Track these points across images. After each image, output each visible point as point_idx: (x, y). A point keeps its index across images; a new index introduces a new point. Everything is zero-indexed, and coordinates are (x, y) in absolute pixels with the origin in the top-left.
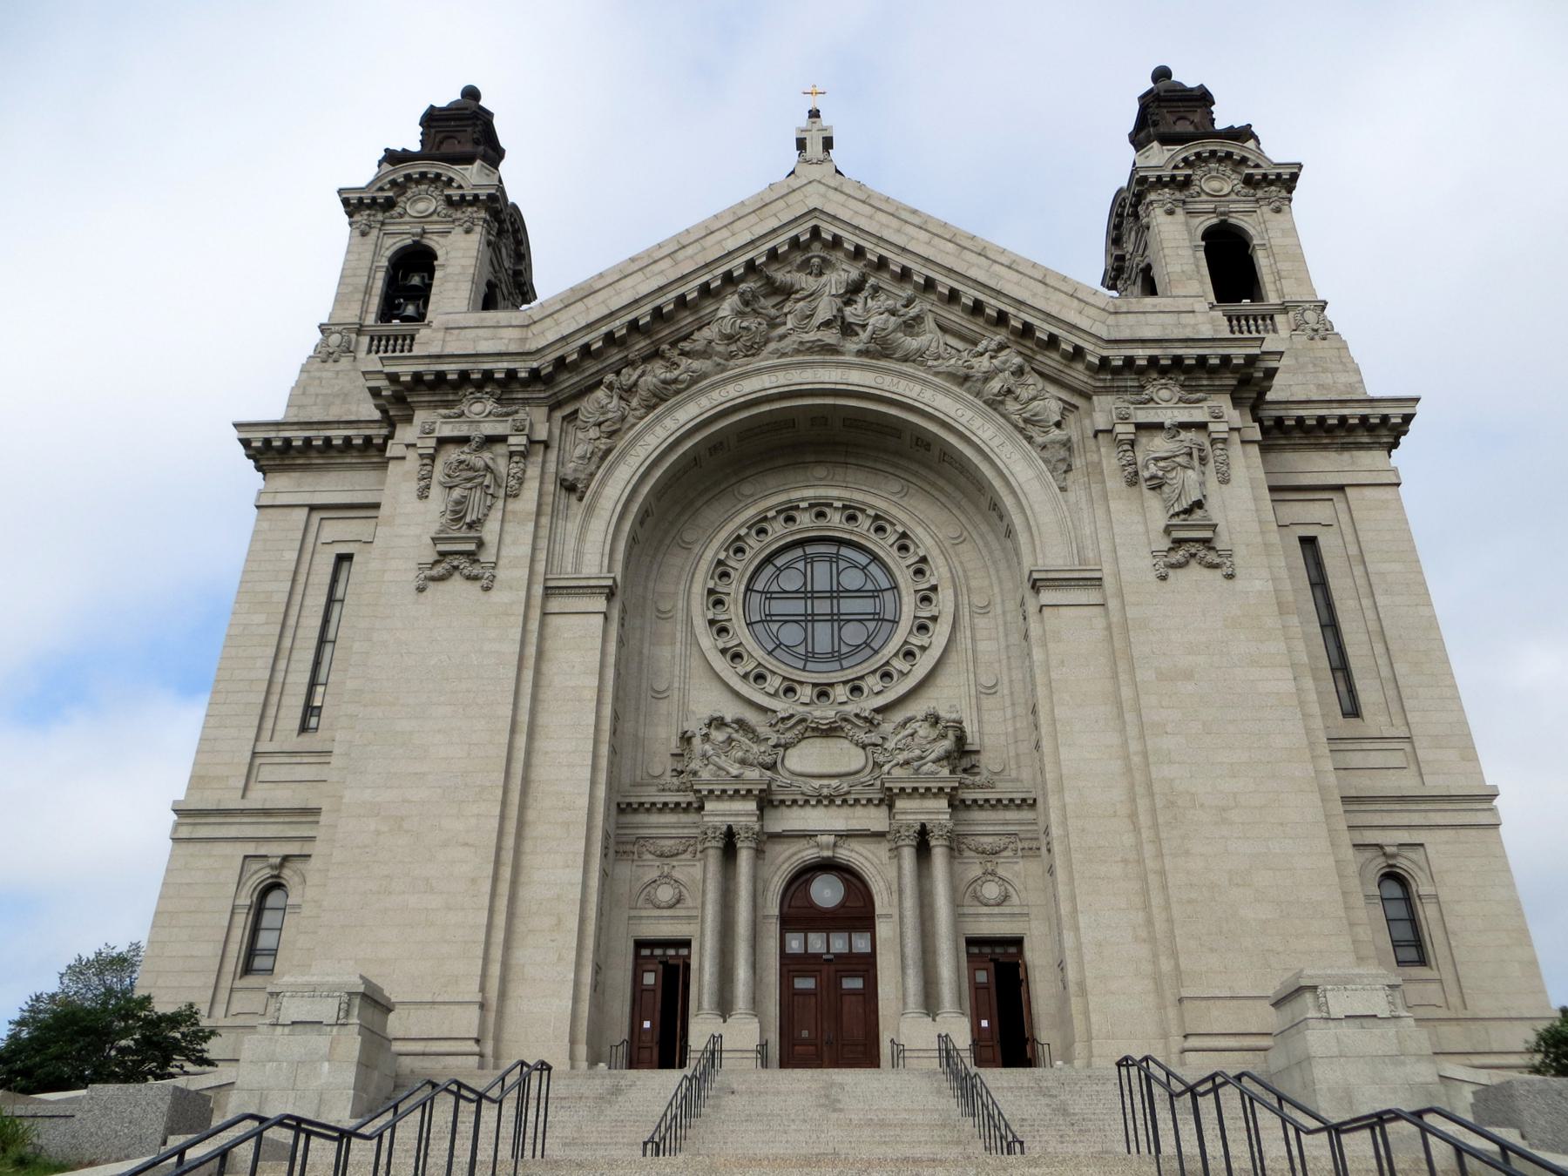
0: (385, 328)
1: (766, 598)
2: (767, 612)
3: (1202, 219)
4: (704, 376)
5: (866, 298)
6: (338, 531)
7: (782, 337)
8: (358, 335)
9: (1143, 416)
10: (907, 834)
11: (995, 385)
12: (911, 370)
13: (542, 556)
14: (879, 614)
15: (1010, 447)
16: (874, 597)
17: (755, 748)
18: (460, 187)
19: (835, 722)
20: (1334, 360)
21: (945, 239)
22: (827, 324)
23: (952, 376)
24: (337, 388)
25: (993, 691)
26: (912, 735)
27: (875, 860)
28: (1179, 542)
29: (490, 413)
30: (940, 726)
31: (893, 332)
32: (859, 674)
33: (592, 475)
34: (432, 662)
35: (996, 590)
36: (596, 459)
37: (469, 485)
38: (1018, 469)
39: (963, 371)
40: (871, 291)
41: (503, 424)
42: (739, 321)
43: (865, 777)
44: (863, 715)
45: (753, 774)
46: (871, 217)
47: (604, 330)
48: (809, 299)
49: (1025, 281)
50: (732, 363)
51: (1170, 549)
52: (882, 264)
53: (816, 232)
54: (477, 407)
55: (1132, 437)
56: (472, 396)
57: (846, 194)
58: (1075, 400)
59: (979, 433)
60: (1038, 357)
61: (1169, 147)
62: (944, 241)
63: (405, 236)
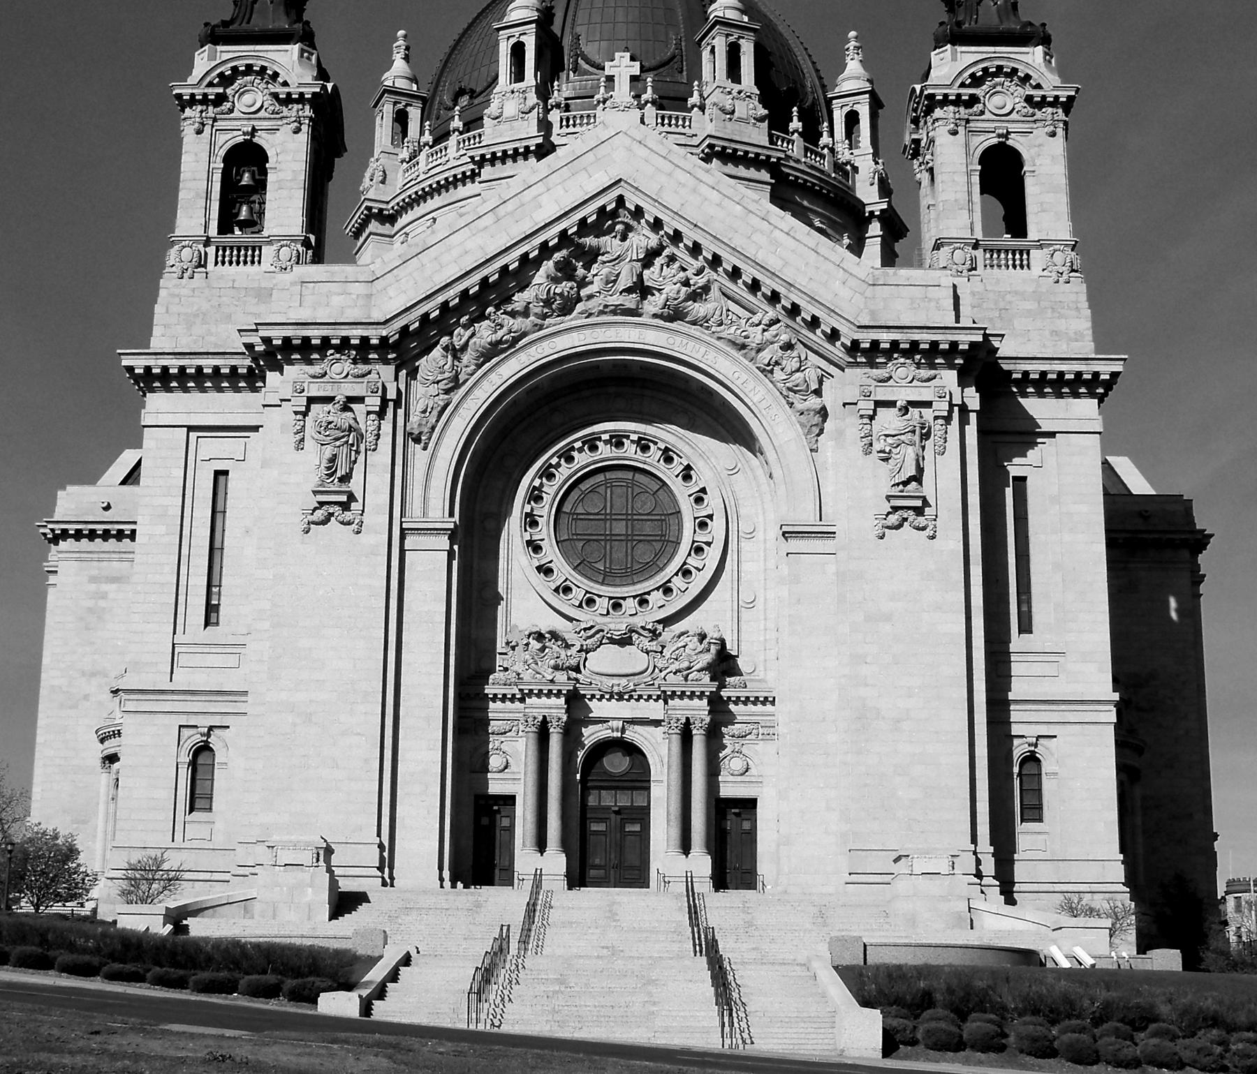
0: (227, 239)
1: (573, 519)
2: (574, 532)
3: (982, 138)
4: (524, 335)
5: (662, 265)
7: (590, 297)
8: (205, 246)
9: (882, 394)
10: (675, 725)
11: (765, 356)
12: (698, 334)
15: (775, 410)
17: (563, 653)
18: (285, 84)
19: (625, 634)
20: (1070, 305)
22: (629, 290)
23: (733, 343)
24: (195, 308)
25: (752, 605)
26: (684, 647)
28: (895, 509)
29: (348, 374)
30: (705, 642)
31: (683, 301)
32: (646, 590)
33: (433, 428)
34: (321, 593)
35: (761, 518)
36: (435, 413)
37: (338, 443)
38: (780, 431)
39: (740, 340)
40: (667, 259)
42: (554, 287)
43: (646, 678)
44: (647, 627)
45: (561, 677)
46: (670, 175)
47: (440, 299)
48: (614, 263)
50: (548, 321)
51: (889, 513)
52: (677, 237)
53: (620, 200)
54: (337, 367)
56: (331, 357)
57: (649, 149)
58: (832, 369)
61: (964, 49)
63: (236, 133)
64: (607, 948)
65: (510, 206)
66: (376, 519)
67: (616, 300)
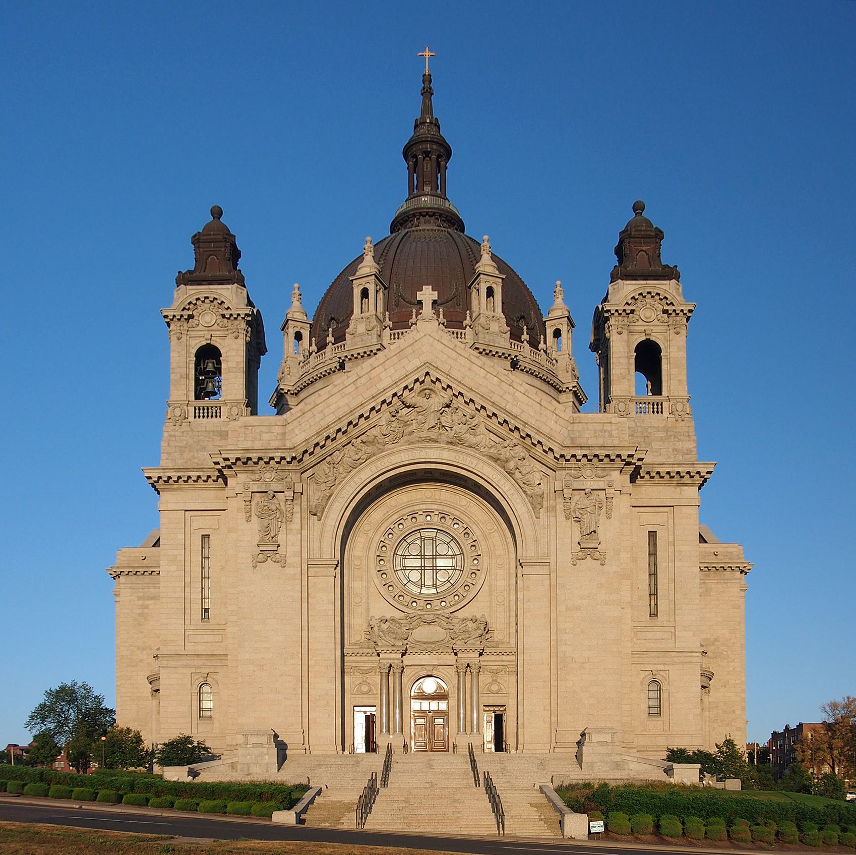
1: (403, 558)
6: (203, 524)
11: (511, 465)
12: (473, 453)
13: (305, 550)
14: (454, 567)
16: (452, 558)
21: (493, 375)
23: (491, 457)
27: (449, 676)
31: (465, 433)
41: (281, 485)
49: (531, 402)
55: (570, 496)
59: (502, 487)
60: (532, 450)
62: (492, 376)
64: (428, 783)
65: (363, 380)
66: (294, 560)
67: (424, 434)
